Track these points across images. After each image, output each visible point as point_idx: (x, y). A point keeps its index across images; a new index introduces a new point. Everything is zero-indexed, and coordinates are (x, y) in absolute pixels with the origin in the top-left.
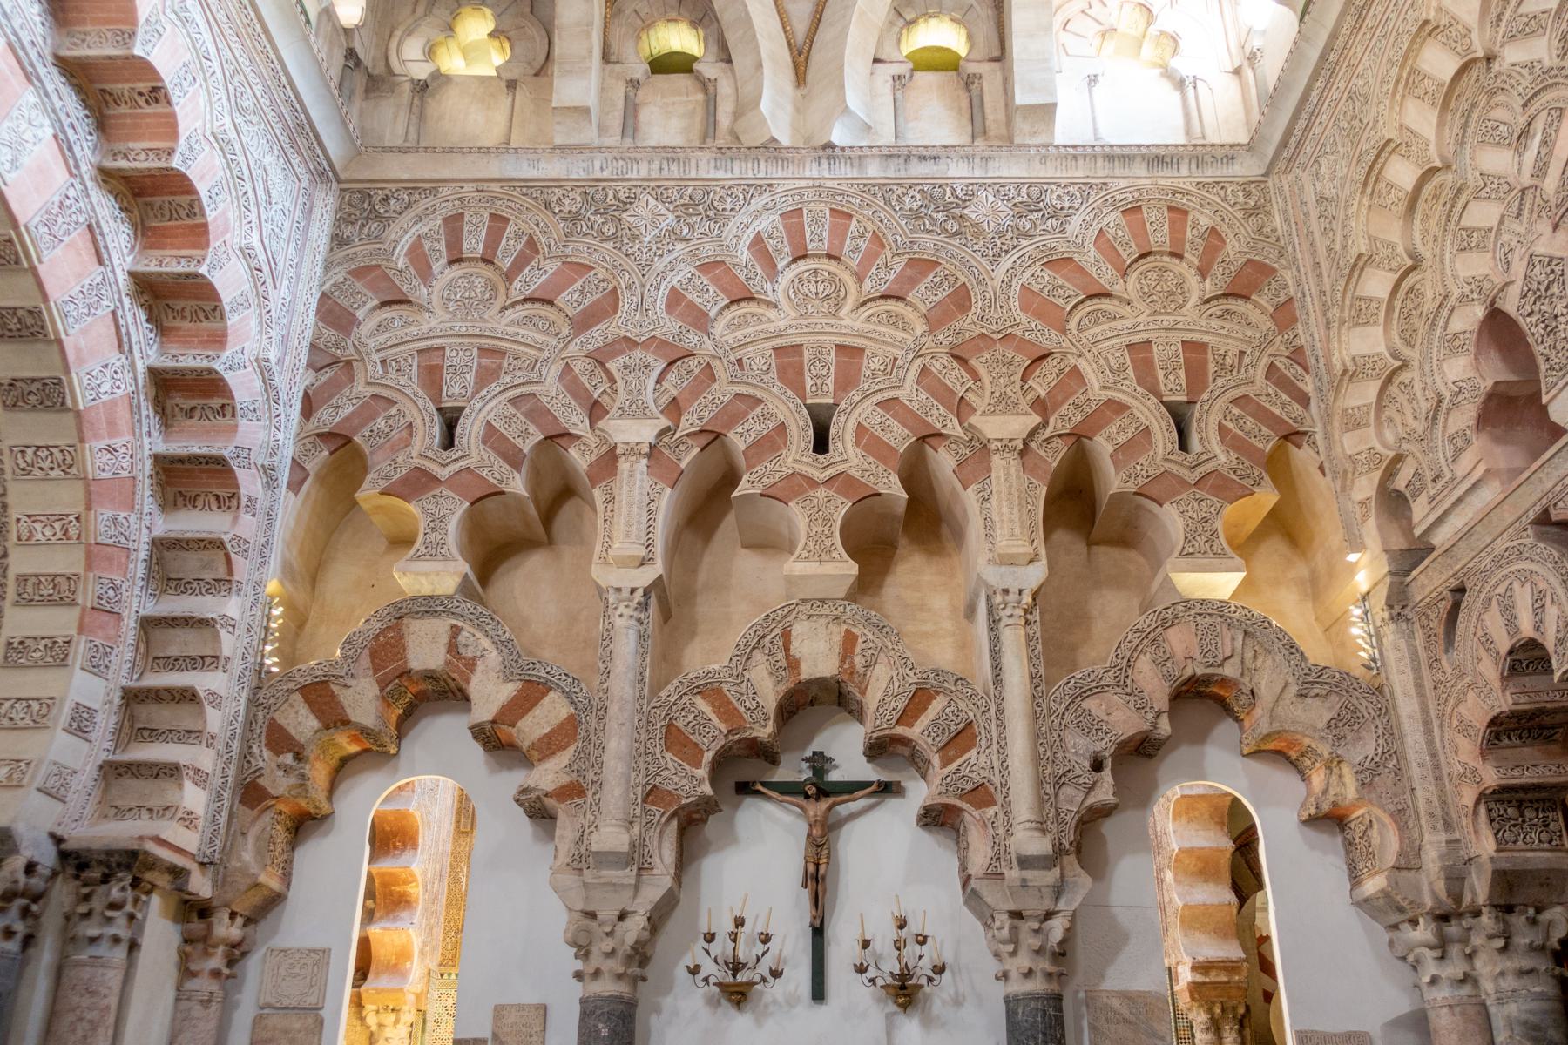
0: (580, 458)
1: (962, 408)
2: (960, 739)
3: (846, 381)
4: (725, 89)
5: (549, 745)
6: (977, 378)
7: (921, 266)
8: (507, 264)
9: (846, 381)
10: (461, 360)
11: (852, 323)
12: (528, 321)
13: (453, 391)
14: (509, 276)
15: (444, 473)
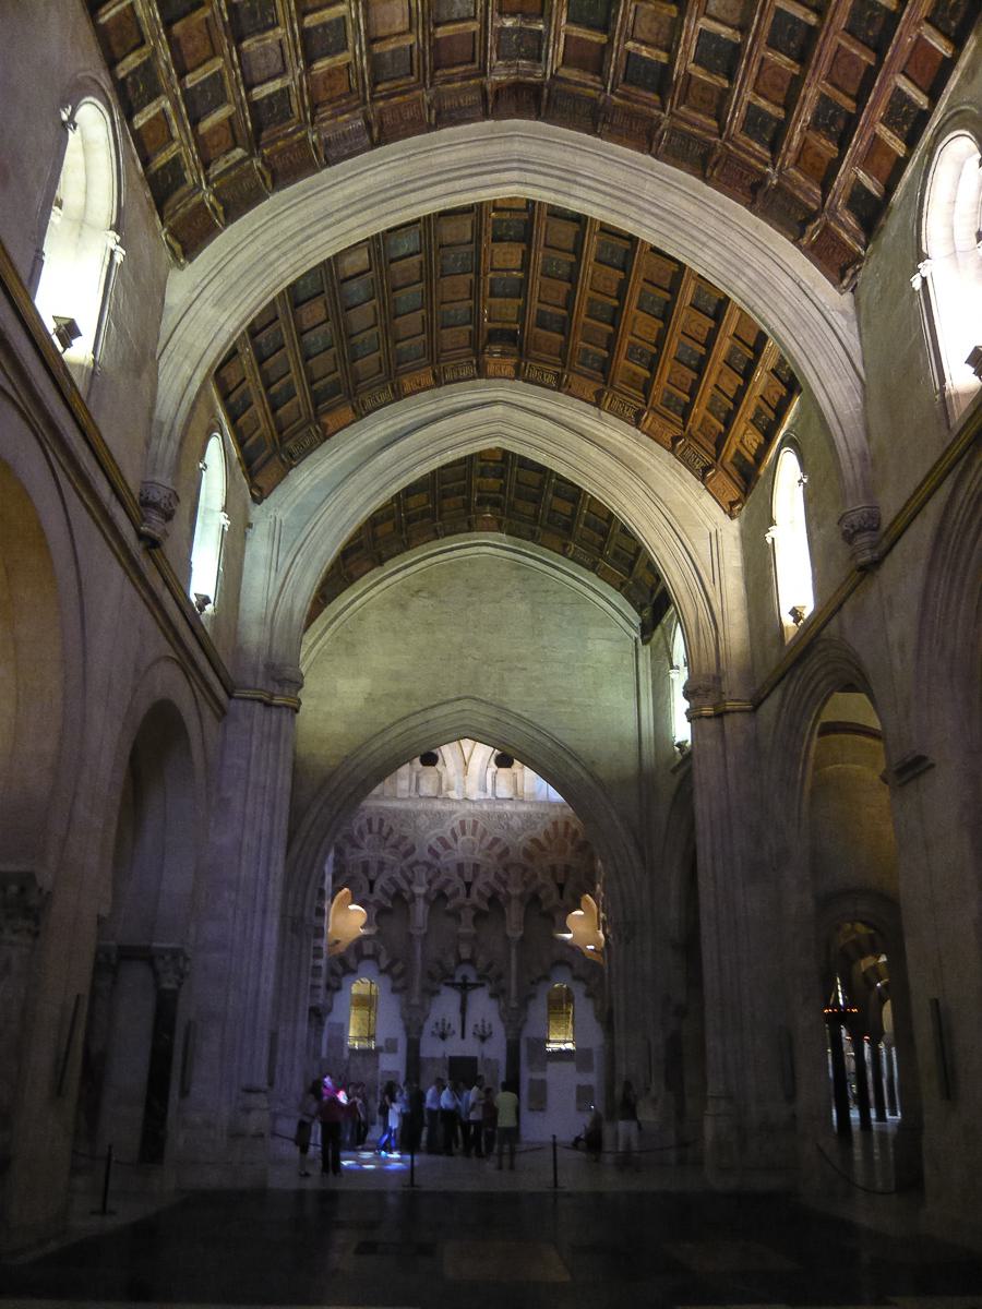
0: (407, 896)
1: (505, 883)
2: (500, 977)
3: (475, 875)
4: (444, 776)
5: (400, 975)
6: (509, 874)
7: (496, 841)
8: (384, 834)
9: (475, 875)
10: (374, 865)
11: (478, 856)
12: (391, 853)
13: (372, 875)
14: (386, 839)
15: (371, 900)
